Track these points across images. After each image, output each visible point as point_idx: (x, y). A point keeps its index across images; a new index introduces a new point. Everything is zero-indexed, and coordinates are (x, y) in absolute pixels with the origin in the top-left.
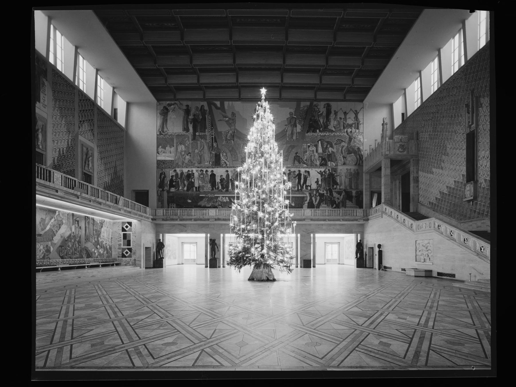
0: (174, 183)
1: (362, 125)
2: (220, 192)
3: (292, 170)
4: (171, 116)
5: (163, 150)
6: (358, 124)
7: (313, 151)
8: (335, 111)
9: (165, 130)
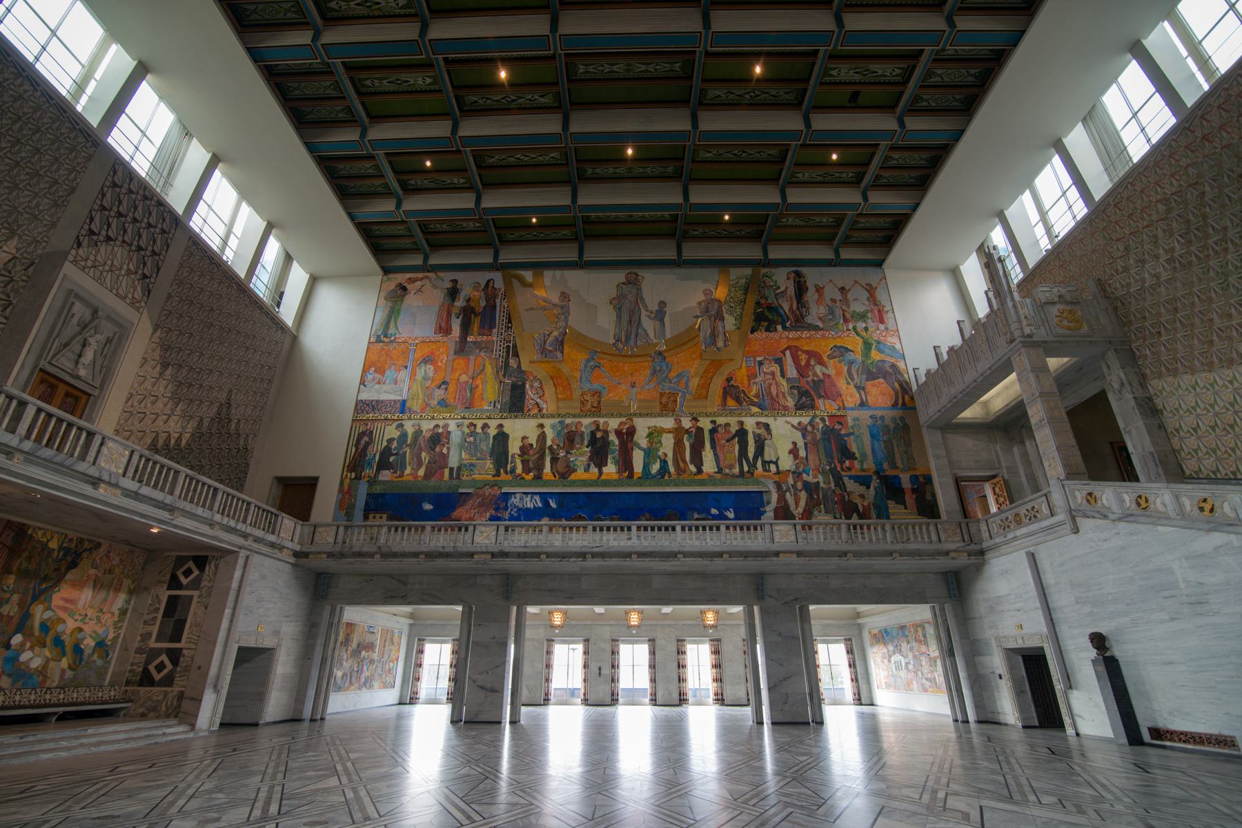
0: (392, 459)
1: (890, 314)
2: (519, 480)
3: (721, 420)
4: (411, 300)
5: (378, 376)
6: (879, 311)
7: (773, 374)
8: (816, 286)
9: (392, 330)
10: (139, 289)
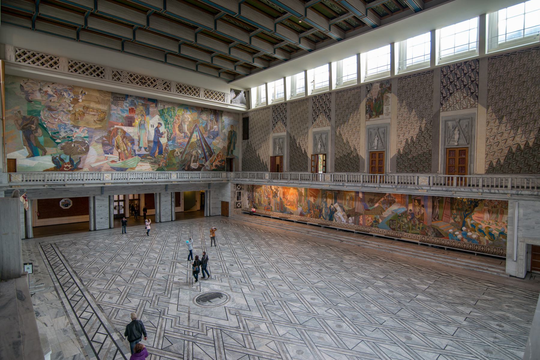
10: (472, 100)
